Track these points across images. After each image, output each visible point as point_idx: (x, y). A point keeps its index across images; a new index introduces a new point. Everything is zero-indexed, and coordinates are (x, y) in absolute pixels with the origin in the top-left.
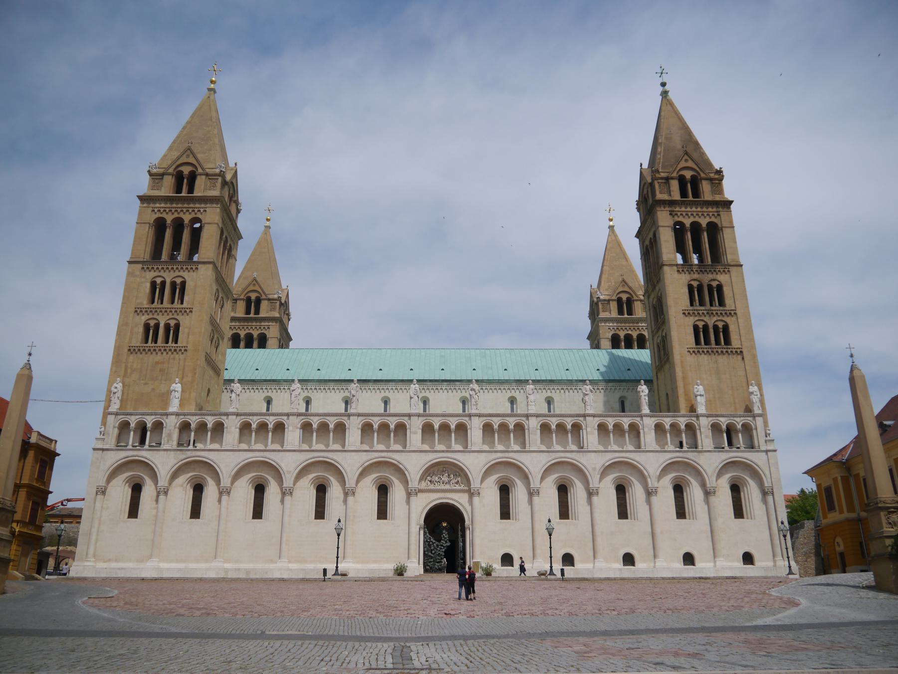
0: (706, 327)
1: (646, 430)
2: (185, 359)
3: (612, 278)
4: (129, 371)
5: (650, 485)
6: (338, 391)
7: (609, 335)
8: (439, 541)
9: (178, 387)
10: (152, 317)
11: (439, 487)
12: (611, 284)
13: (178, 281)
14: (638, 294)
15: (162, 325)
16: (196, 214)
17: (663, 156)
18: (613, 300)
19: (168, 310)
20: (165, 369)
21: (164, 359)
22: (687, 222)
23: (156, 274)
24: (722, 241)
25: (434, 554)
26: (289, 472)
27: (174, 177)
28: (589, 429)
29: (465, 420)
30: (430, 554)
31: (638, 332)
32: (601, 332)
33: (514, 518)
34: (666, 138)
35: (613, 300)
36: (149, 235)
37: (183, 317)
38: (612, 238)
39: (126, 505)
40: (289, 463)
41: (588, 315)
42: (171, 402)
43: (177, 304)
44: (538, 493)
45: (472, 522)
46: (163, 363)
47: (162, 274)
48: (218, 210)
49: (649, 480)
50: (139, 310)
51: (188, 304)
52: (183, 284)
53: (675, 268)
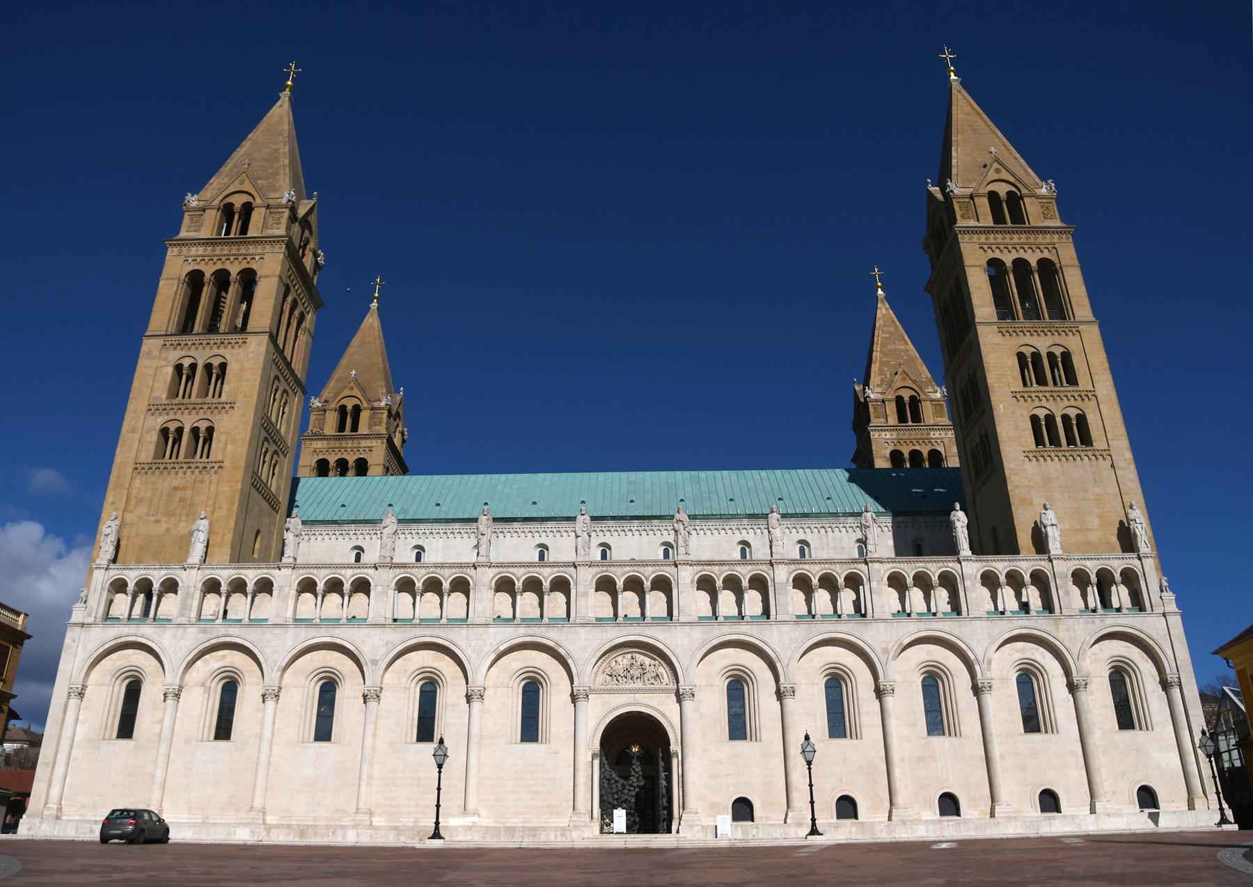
0: (1050, 419)
1: (968, 583)
2: (218, 483)
3: (886, 369)
4: (133, 502)
5: (979, 676)
6: (465, 536)
7: (887, 453)
8: (627, 778)
9: (203, 525)
10: (173, 417)
11: (627, 686)
12: (886, 377)
13: (216, 362)
14: (927, 390)
15: (187, 430)
16: (248, 263)
18: (890, 401)
19: (198, 407)
20: (187, 498)
21: (187, 482)
22: (1008, 259)
23: (183, 353)
24: (1064, 287)
25: (617, 799)
26: (375, 662)
27: (220, 211)
28: (874, 584)
29: (668, 571)
30: (611, 800)
31: (929, 448)
32: (873, 448)
33: (754, 737)
35: (890, 401)
36: (178, 296)
37: (218, 417)
38: (881, 312)
39: (115, 717)
40: (374, 645)
41: (851, 426)
42: (191, 549)
44: (794, 692)
45: (682, 745)
46: (185, 488)
47: (192, 353)
48: (281, 256)
49: (977, 667)
50: (153, 408)
51: (228, 397)
53: (995, 327)
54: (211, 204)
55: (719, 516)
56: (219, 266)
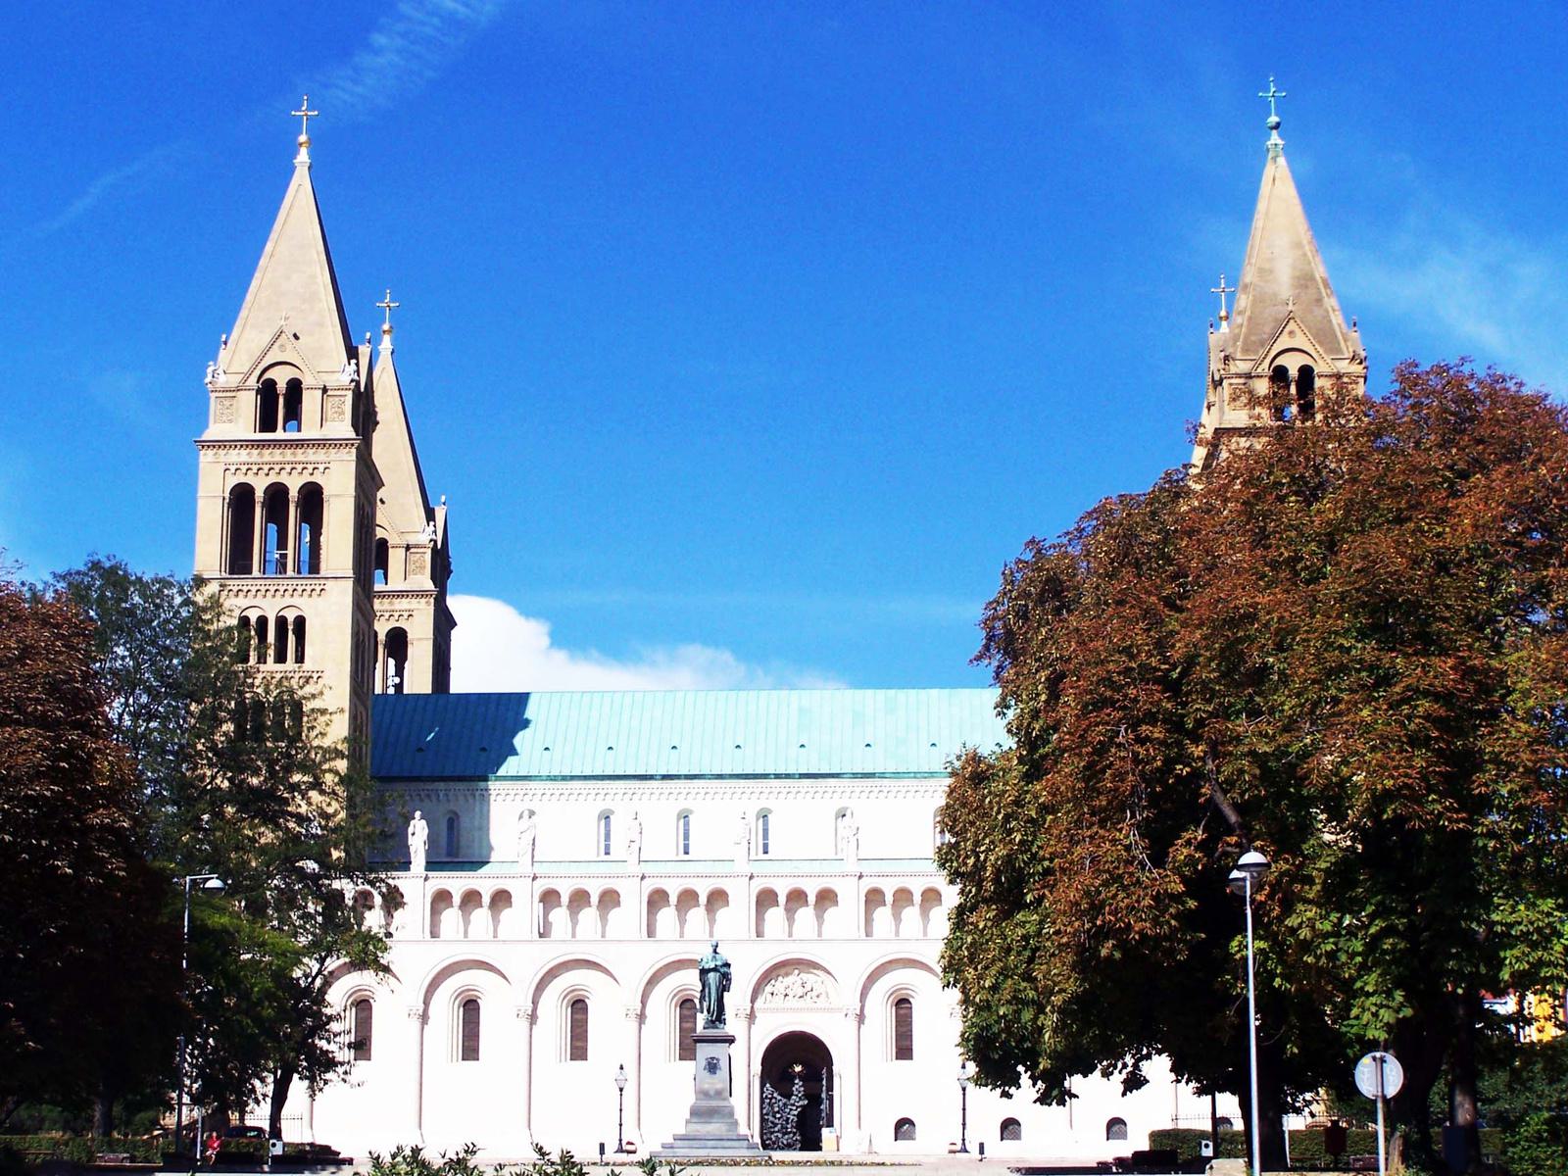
16: (312, 474)
17: (1250, 318)
25: (779, 1119)
30: (771, 1119)
34: (1261, 271)
43: (290, 664)
52: (300, 622)
54: (247, 384)
55: (912, 775)
56: (273, 478)
